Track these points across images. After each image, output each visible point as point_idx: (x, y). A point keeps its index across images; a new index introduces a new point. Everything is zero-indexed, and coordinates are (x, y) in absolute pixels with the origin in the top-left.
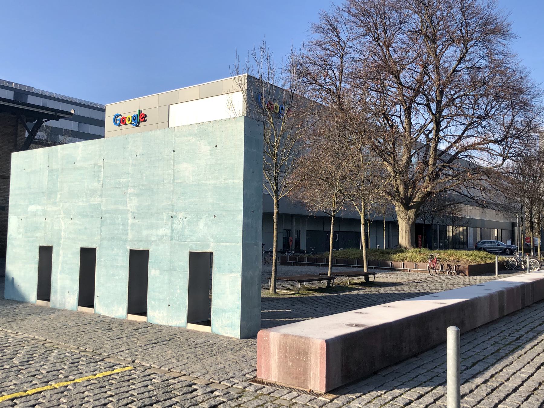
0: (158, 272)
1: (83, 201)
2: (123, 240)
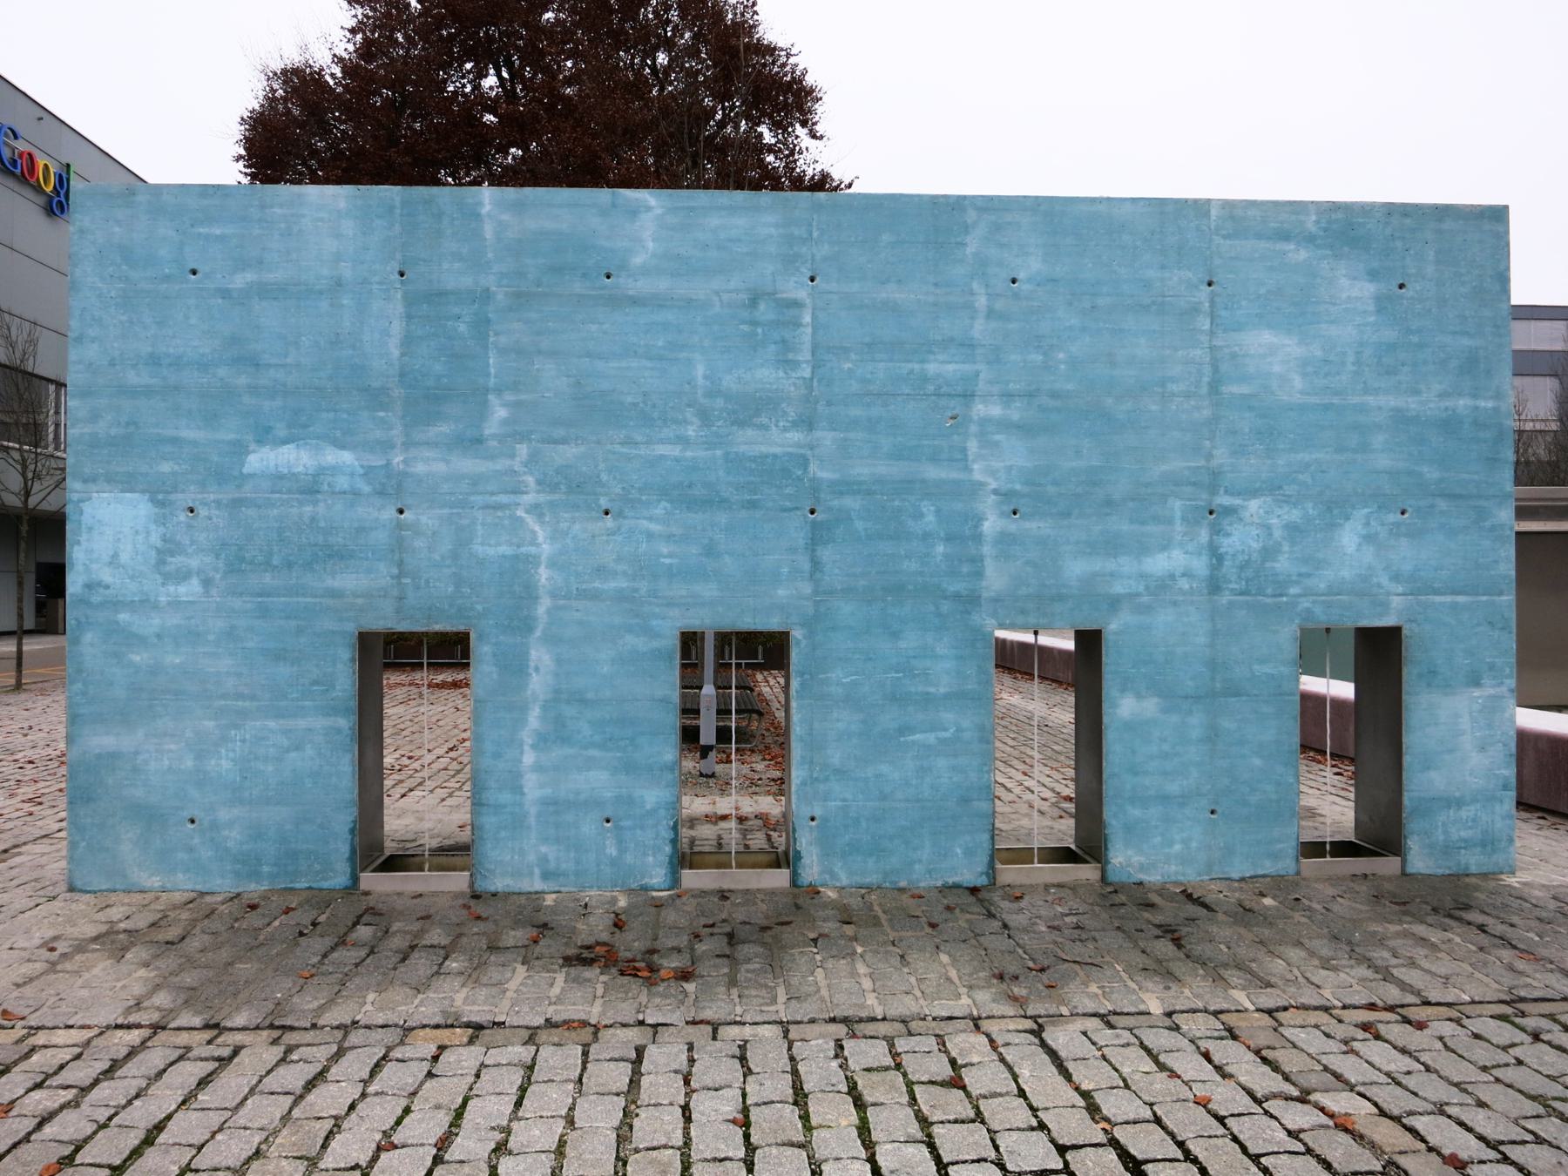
0: (1150, 706)
1: (683, 441)
2: (957, 596)
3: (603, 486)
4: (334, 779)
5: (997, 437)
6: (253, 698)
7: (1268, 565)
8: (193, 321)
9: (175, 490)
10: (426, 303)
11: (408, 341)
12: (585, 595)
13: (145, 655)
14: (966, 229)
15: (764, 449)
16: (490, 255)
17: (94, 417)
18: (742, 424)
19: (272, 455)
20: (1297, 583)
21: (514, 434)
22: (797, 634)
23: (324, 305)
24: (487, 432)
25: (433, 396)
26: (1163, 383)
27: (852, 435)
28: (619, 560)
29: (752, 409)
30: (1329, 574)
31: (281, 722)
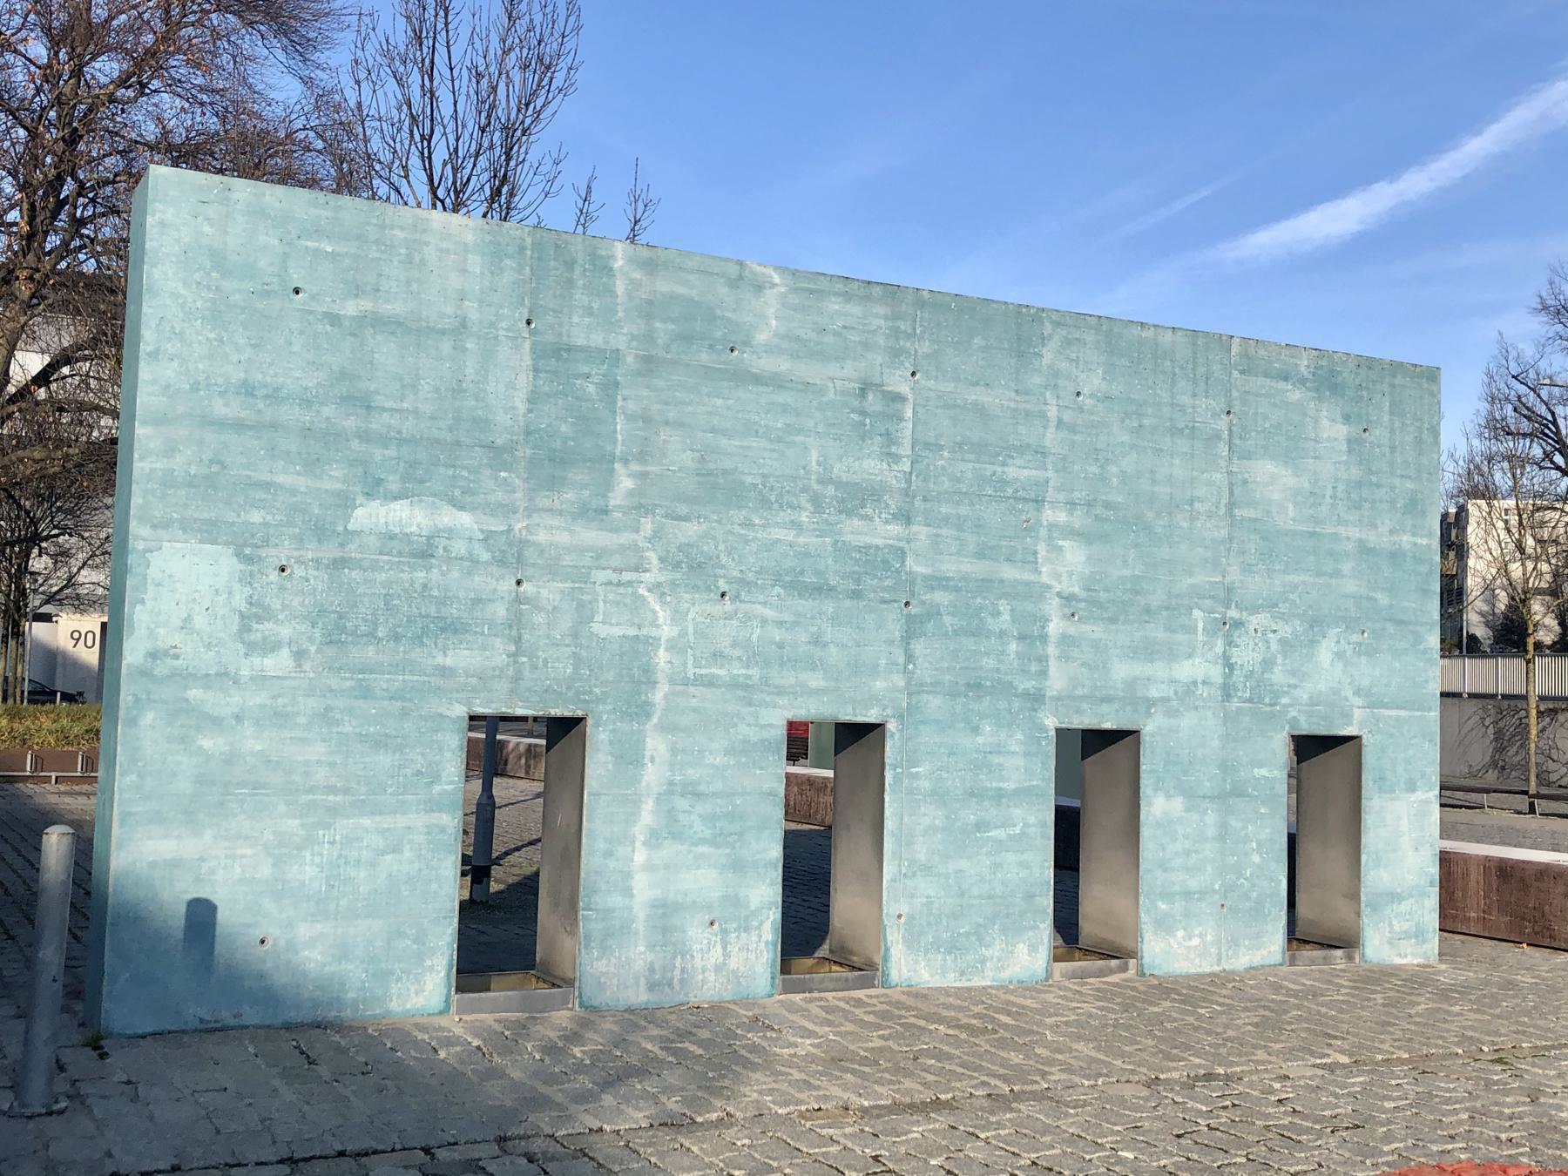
0: (1177, 805)
1: (796, 526)
2: (1026, 695)
3: (723, 567)
4: (434, 886)
5: (1060, 543)
6: (346, 791)
7: (1266, 676)
8: (296, 348)
9: (266, 542)
10: (554, 356)
11: (533, 399)
12: (701, 681)
13: (220, 741)
14: (1043, 340)
15: (868, 540)
16: (621, 314)
17: (170, 451)
18: (849, 513)
19: (383, 511)
20: (1287, 693)
21: (640, 507)
22: (891, 726)
23: (446, 346)
24: (612, 503)
25: (557, 459)
26: (1191, 502)
27: (944, 531)
28: (734, 645)
29: (858, 498)
30: (1308, 685)
31: (378, 819)
